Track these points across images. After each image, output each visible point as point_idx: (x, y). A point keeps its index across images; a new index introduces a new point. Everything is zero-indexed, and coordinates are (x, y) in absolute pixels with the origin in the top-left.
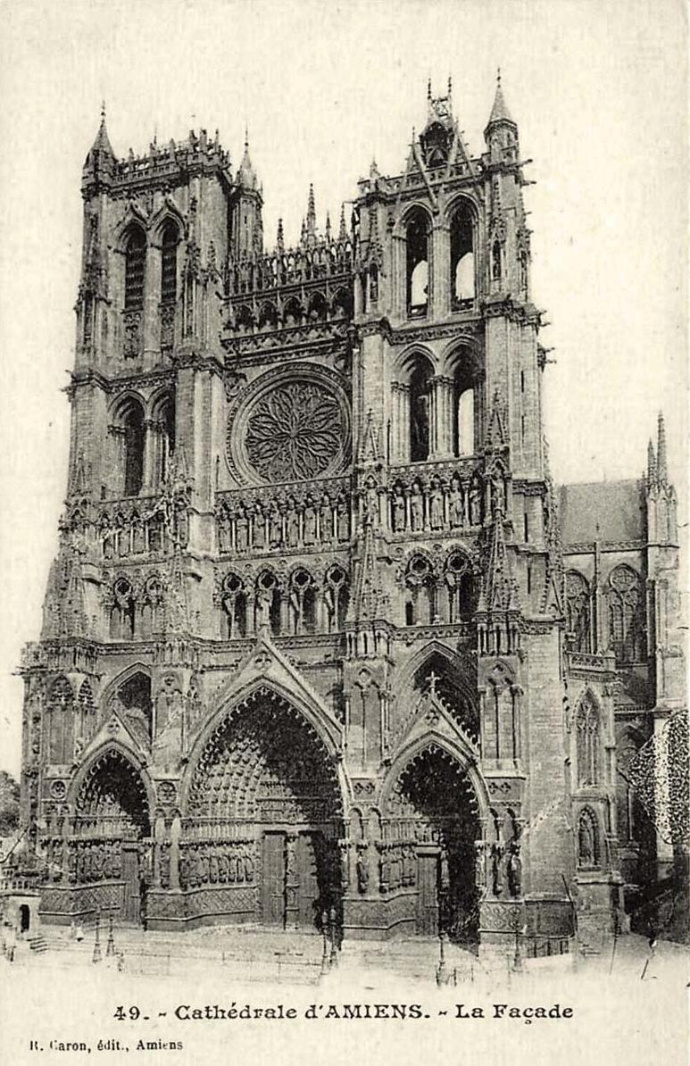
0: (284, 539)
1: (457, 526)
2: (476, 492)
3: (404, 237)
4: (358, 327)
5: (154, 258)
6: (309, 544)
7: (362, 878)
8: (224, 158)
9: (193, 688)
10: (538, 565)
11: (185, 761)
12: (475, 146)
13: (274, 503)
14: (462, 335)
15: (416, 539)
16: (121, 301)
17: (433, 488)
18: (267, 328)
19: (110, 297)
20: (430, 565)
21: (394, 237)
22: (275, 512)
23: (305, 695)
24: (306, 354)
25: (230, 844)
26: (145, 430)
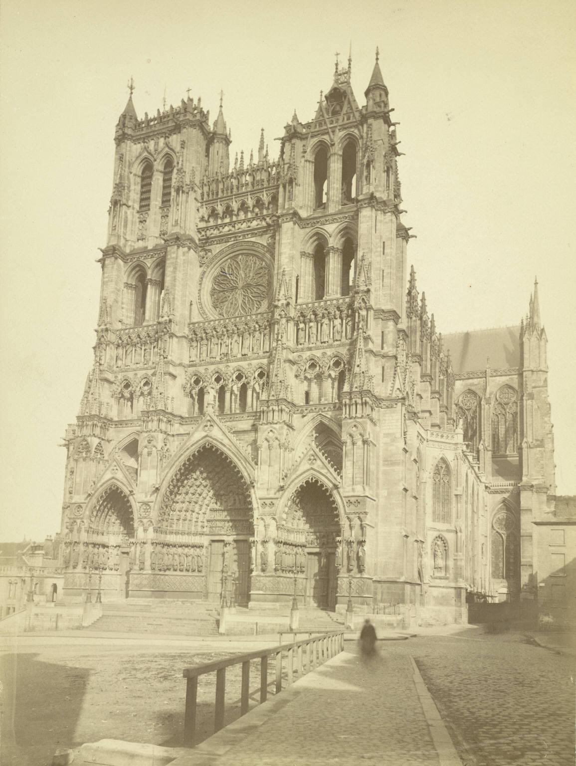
0: (229, 352)
1: (337, 340)
2: (349, 319)
3: (314, 161)
4: (279, 217)
5: (158, 180)
6: (245, 355)
7: (264, 563)
8: (205, 116)
9: (165, 445)
10: (390, 364)
11: (157, 489)
12: (361, 101)
13: (224, 330)
14: (346, 220)
15: (310, 349)
16: (137, 206)
17: (323, 317)
18: (227, 220)
19: (130, 203)
20: (320, 366)
21: (306, 161)
22: (224, 335)
23: (233, 447)
24: (249, 236)
25: (187, 546)
26: (147, 285)
